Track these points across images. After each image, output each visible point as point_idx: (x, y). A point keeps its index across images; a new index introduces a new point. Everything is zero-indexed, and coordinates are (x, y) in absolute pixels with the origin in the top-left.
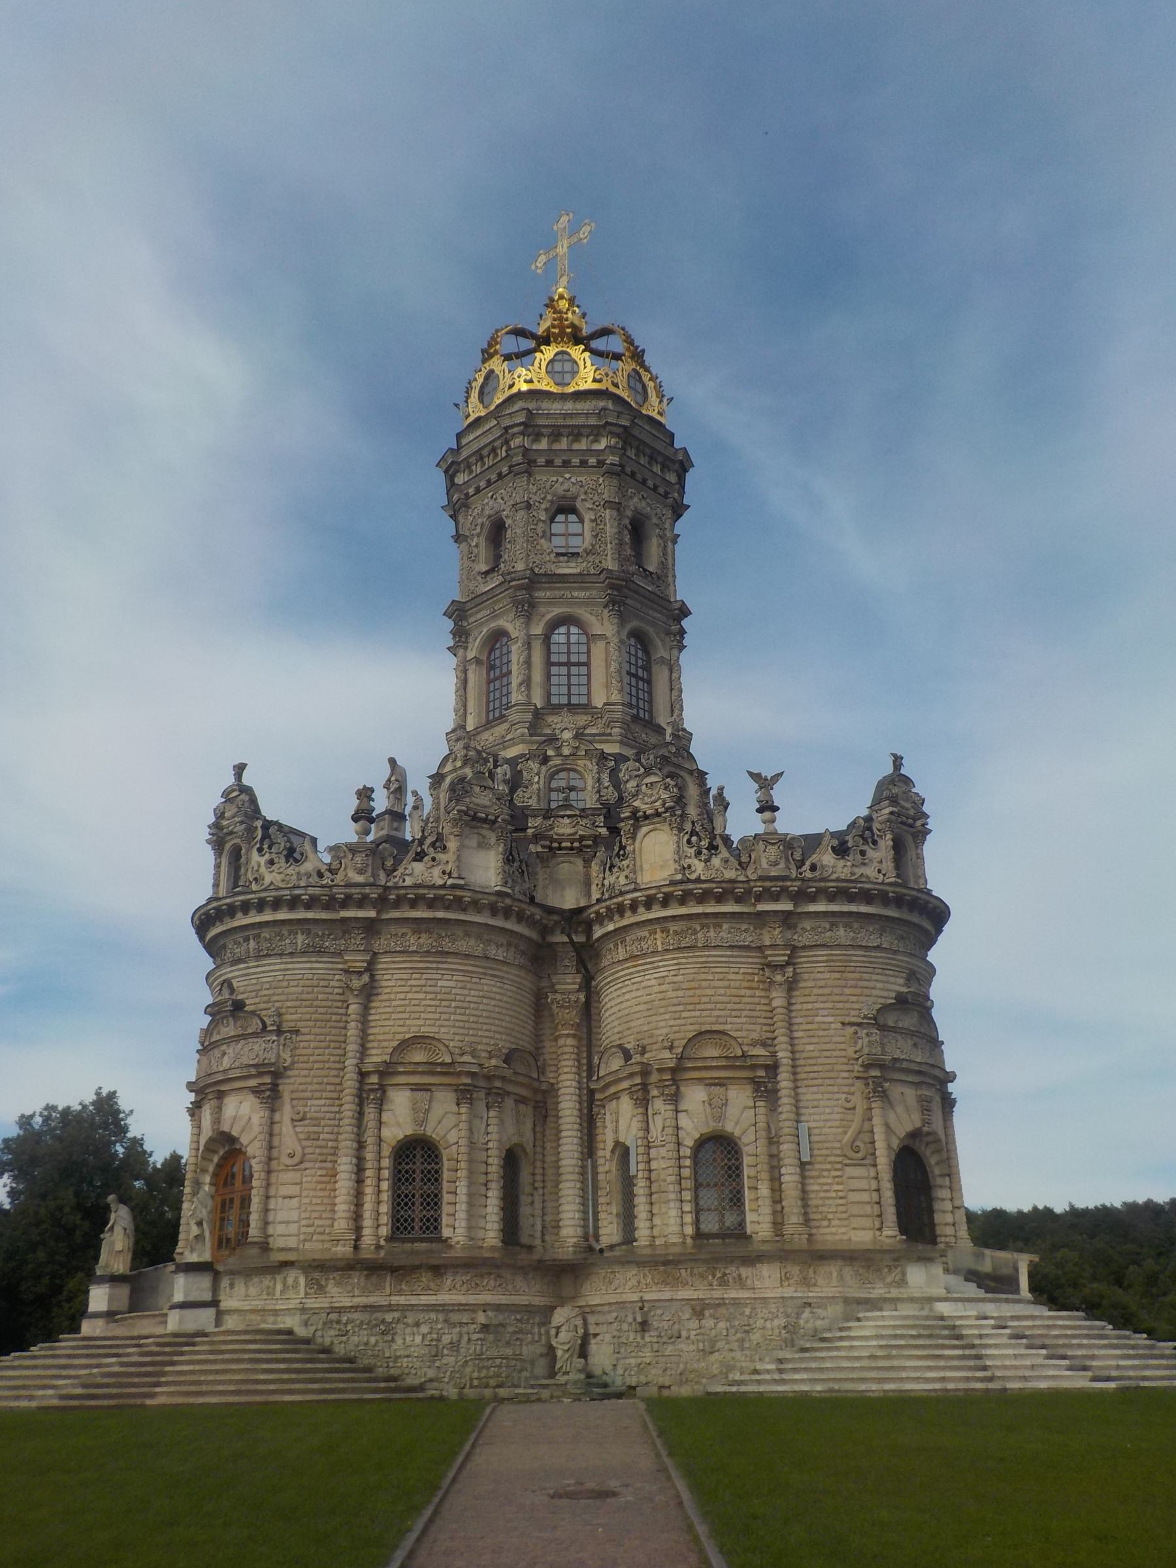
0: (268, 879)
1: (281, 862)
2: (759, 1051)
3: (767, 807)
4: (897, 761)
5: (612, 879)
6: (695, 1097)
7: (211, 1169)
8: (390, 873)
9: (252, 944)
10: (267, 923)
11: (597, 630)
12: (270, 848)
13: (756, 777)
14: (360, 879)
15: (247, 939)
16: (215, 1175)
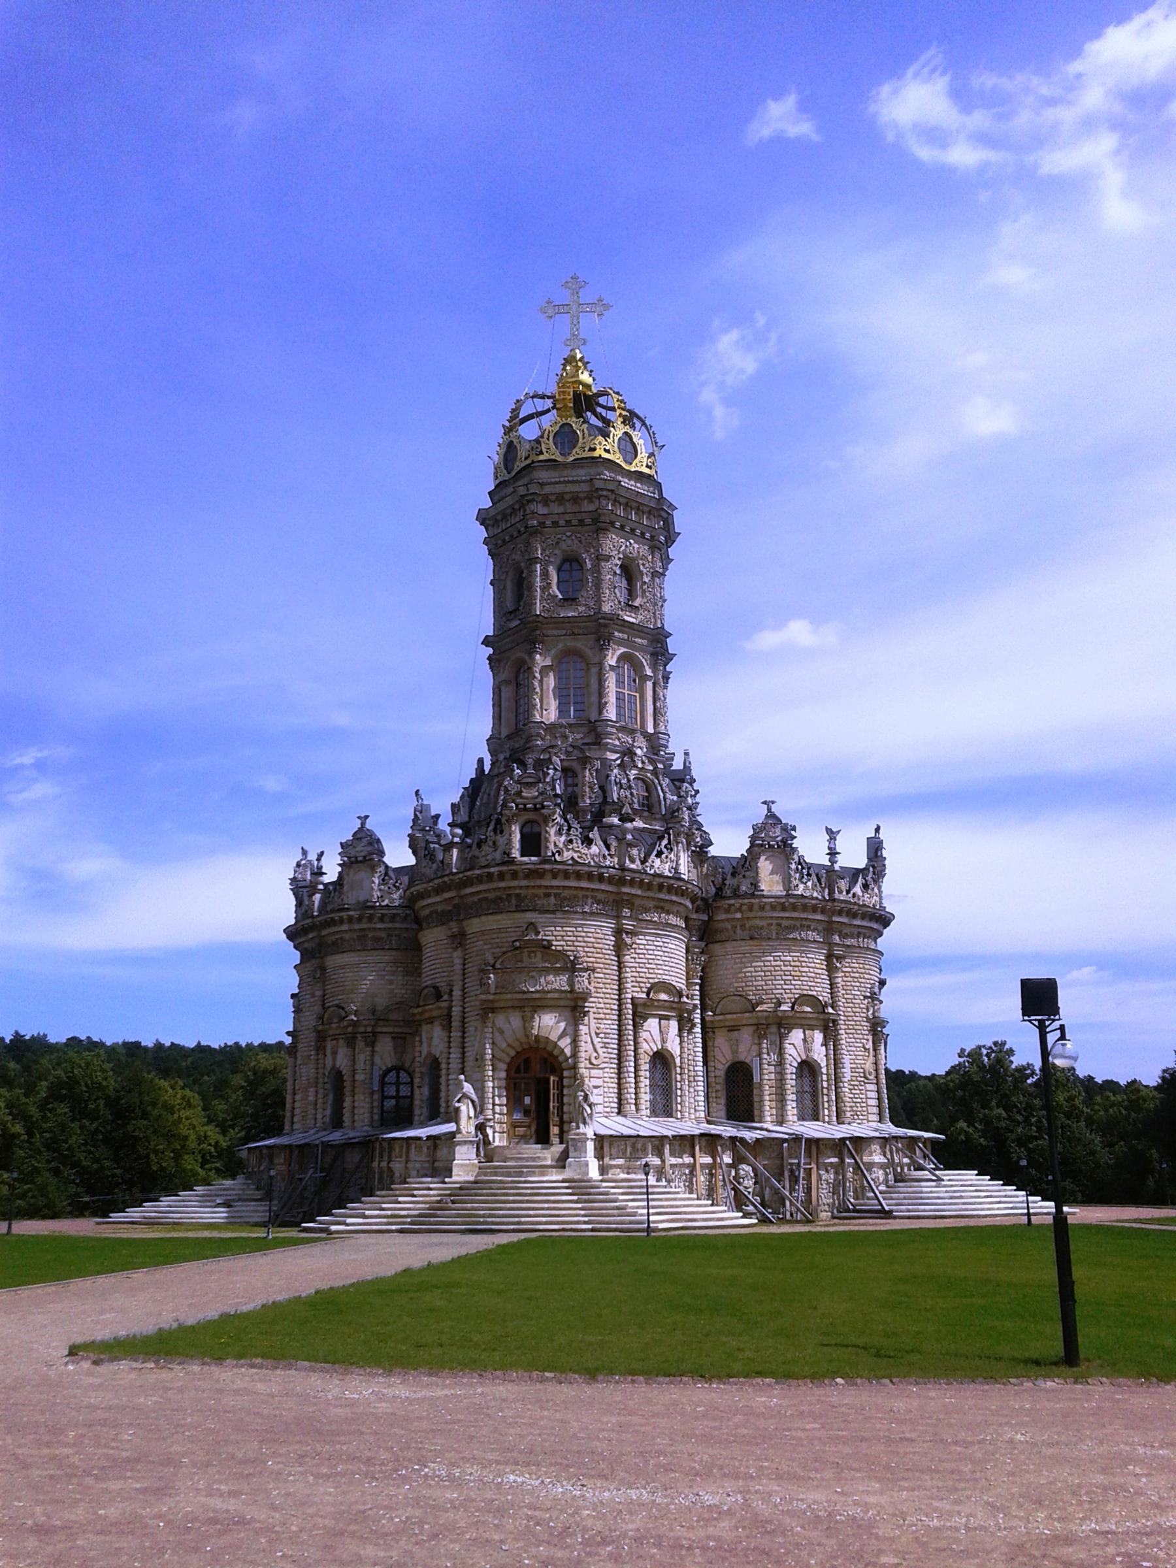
0: (567, 855)
1: (577, 844)
2: (830, 1010)
3: (833, 853)
4: (877, 830)
5: (735, 882)
6: (796, 1036)
7: (508, 1060)
8: (643, 862)
9: (552, 900)
10: (570, 887)
12: (569, 830)
13: (829, 831)
14: (633, 866)
15: (547, 895)
16: (509, 1065)
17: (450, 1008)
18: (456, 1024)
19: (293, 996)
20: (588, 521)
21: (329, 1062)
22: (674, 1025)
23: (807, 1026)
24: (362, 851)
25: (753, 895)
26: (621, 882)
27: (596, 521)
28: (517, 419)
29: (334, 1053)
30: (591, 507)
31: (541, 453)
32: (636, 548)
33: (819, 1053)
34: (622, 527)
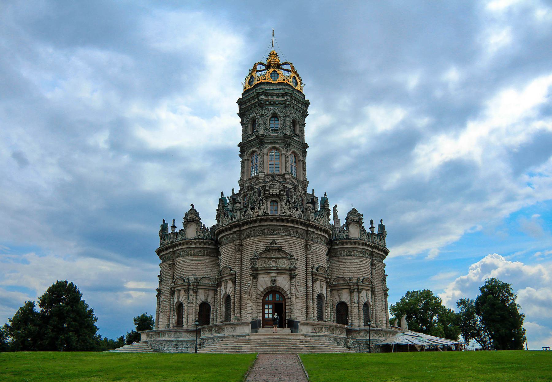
0: (288, 213)
6: (363, 294)
11: (301, 158)
17: (235, 275)
18: (238, 281)
19: (159, 276)
20: (282, 103)
21: (176, 300)
22: (325, 284)
23: (367, 290)
24: (193, 217)
25: (347, 239)
26: (308, 226)
27: (285, 104)
28: (254, 70)
29: (179, 296)
30: (283, 99)
31: (265, 79)
32: (298, 116)
33: (370, 301)
34: (293, 107)
